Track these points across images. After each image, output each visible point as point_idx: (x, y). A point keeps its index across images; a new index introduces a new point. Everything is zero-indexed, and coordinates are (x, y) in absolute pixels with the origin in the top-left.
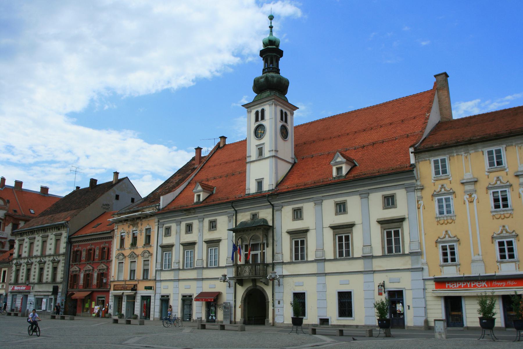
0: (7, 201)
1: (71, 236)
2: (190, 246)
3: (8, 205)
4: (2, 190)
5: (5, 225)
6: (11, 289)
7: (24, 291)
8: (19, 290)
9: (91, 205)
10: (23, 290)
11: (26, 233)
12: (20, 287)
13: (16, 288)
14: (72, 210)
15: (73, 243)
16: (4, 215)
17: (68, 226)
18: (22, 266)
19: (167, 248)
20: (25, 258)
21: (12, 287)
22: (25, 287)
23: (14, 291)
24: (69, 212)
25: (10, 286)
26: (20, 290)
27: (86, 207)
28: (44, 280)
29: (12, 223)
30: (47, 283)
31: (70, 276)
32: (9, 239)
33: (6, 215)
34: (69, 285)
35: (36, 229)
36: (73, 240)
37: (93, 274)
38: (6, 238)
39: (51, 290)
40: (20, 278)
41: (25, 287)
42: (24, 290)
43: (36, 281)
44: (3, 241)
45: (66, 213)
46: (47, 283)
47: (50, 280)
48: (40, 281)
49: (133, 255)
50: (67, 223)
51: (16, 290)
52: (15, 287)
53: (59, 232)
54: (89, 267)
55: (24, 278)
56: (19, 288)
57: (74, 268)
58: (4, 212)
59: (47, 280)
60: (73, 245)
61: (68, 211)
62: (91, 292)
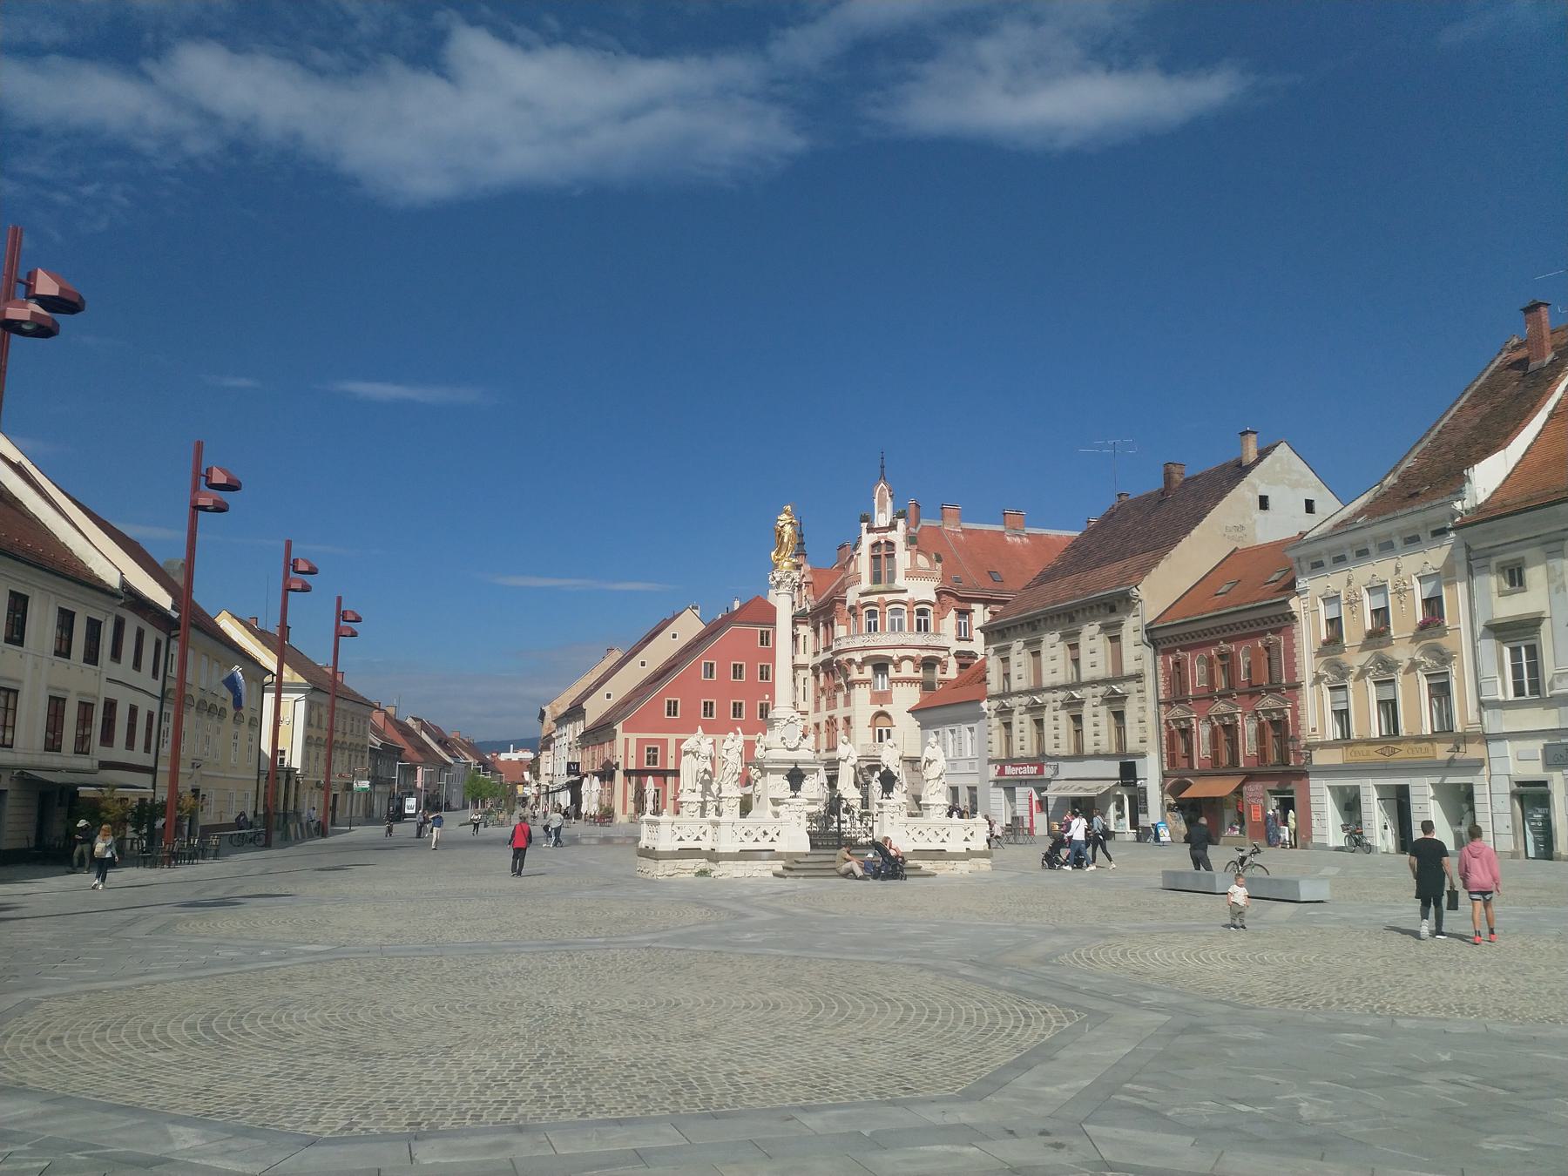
0: (934, 557)
1: (1151, 623)
3: (939, 565)
4: (917, 532)
5: (941, 616)
7: (1034, 777)
9: (1193, 532)
10: (1030, 774)
11: (1015, 627)
13: (1009, 770)
14: (1133, 553)
15: (1159, 644)
16: (934, 593)
17: (1140, 597)
18: (1016, 713)
20: (1020, 693)
21: (999, 767)
22: (1036, 768)
24: (1128, 561)
25: (992, 767)
26: (1023, 775)
27: (1180, 541)
28: (1089, 748)
29: (955, 610)
30: (1097, 756)
31: (1165, 734)
32: (952, 651)
33: (939, 593)
34: (1165, 759)
35: (1042, 616)
36: (1158, 635)
37: (1243, 725)
38: (947, 649)
39: (1117, 775)
40: (1016, 743)
41: (1036, 768)
42: (1034, 774)
43: (1066, 749)
44: (941, 654)
45: (1119, 566)
46: (1097, 756)
47: (1107, 742)
48: (1079, 756)
50: (1135, 590)
53: (1114, 618)
54: (1221, 707)
57: (1172, 712)
58: (935, 584)
60: (1160, 647)
61: (1123, 558)
62: (1245, 776)
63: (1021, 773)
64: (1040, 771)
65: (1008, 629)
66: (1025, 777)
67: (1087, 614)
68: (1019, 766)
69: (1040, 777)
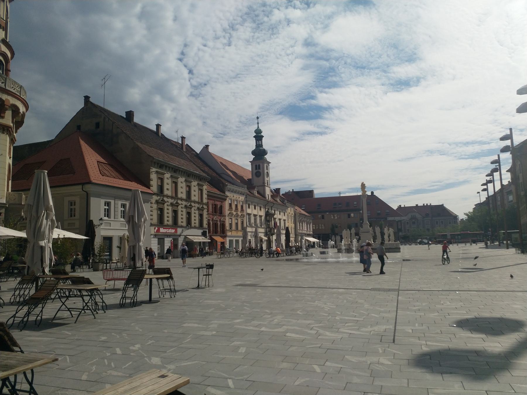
2: (255, 216)
6: (155, 230)
7: (173, 234)
8: (166, 233)
10: (171, 233)
12: (167, 230)
13: (162, 230)
19: (249, 215)
21: (157, 228)
22: (174, 230)
23: (160, 233)
25: (153, 228)
26: (168, 233)
41: (174, 230)
42: (173, 233)
49: (237, 215)
51: (162, 232)
52: (161, 229)
55: (170, 219)
56: (166, 230)
59: (195, 225)
63: (167, 232)
64: (176, 231)
65: (166, 167)
66: (169, 234)
67: (193, 177)
68: (167, 229)
69: (175, 234)
